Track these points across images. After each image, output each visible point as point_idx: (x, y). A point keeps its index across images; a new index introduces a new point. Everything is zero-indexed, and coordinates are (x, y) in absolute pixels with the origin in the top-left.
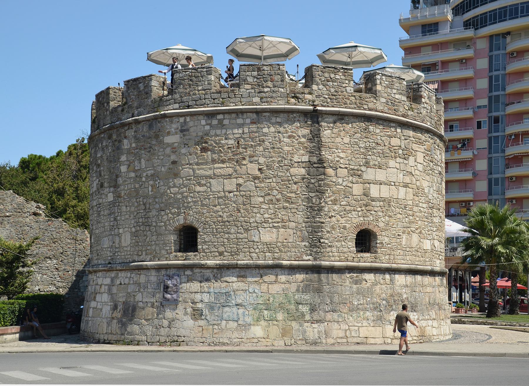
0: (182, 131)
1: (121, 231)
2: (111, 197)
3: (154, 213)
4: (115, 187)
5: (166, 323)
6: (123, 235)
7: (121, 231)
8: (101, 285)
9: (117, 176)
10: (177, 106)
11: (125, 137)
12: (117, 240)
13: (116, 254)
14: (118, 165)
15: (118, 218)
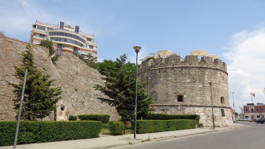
0: (220, 74)
1: (206, 96)
2: (200, 86)
3: (216, 92)
4: (203, 83)
5: (224, 121)
6: (207, 97)
7: (206, 96)
8: (198, 110)
9: (203, 81)
10: (219, 68)
11: (206, 71)
12: (204, 98)
13: (204, 102)
14: (204, 78)
15: (205, 92)
